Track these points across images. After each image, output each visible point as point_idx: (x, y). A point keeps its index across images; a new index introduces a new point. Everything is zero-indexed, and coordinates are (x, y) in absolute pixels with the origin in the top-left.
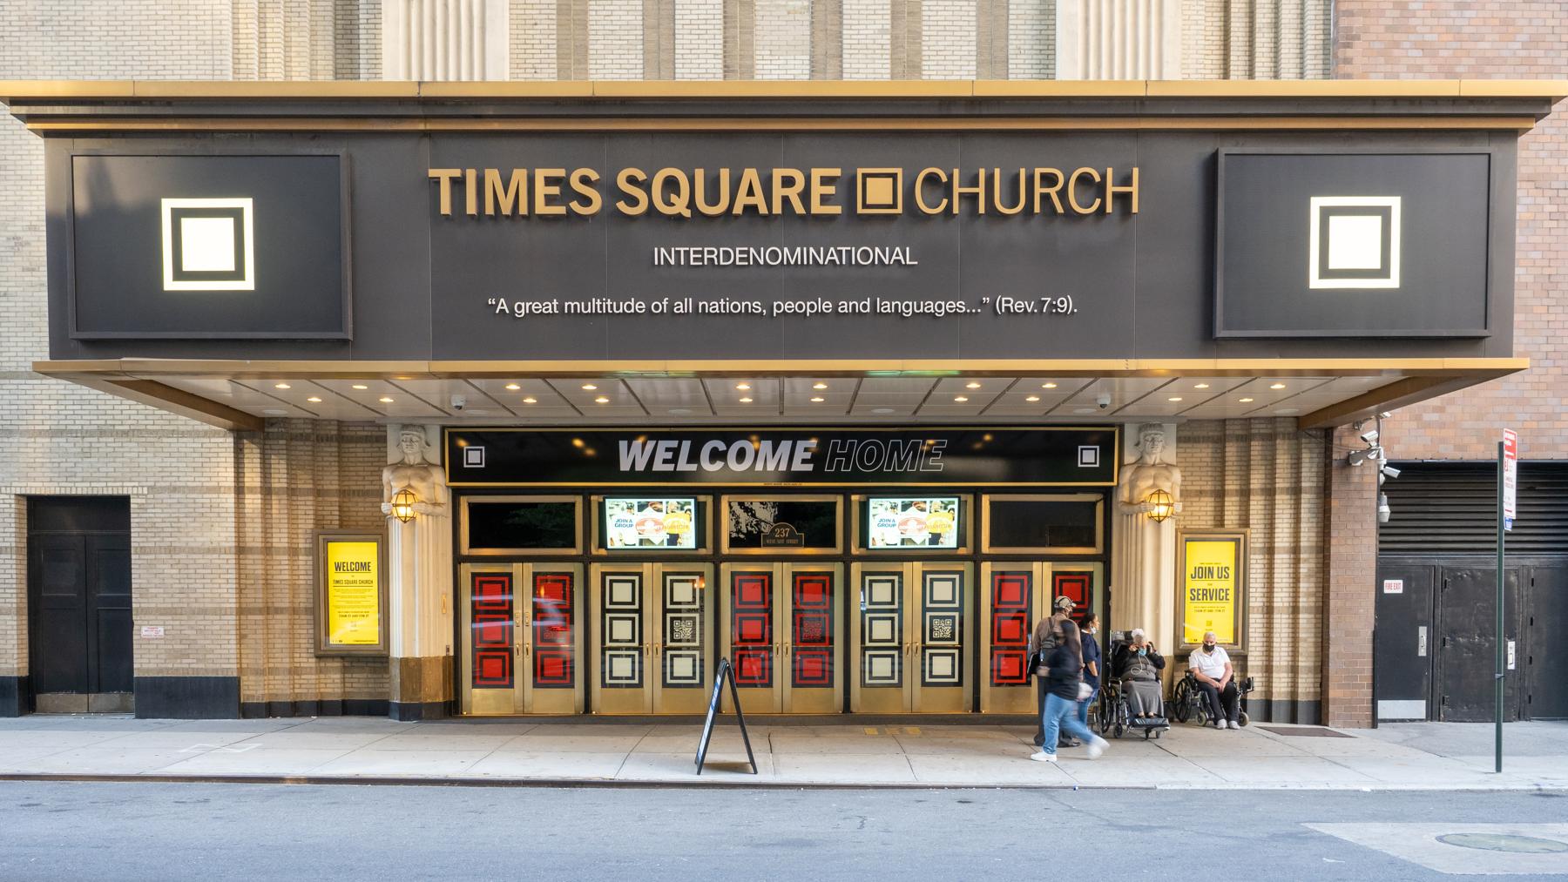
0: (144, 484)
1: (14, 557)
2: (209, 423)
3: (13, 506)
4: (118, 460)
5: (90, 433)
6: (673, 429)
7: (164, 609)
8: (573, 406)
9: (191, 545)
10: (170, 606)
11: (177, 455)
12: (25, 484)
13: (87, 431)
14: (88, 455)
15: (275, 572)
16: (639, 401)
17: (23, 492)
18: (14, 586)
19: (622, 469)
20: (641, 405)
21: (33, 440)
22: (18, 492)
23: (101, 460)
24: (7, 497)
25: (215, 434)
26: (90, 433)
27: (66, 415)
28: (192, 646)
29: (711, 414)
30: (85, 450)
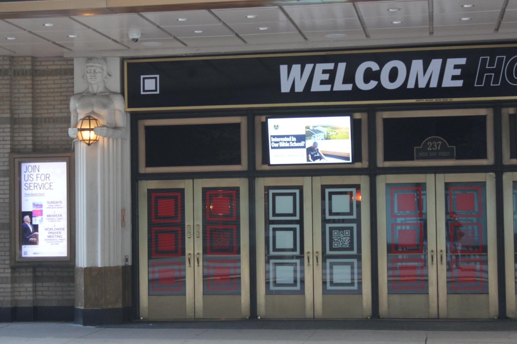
6: (328, 53)
8: (237, 35)
16: (297, 27)
19: (283, 90)
20: (300, 32)
29: (365, 37)
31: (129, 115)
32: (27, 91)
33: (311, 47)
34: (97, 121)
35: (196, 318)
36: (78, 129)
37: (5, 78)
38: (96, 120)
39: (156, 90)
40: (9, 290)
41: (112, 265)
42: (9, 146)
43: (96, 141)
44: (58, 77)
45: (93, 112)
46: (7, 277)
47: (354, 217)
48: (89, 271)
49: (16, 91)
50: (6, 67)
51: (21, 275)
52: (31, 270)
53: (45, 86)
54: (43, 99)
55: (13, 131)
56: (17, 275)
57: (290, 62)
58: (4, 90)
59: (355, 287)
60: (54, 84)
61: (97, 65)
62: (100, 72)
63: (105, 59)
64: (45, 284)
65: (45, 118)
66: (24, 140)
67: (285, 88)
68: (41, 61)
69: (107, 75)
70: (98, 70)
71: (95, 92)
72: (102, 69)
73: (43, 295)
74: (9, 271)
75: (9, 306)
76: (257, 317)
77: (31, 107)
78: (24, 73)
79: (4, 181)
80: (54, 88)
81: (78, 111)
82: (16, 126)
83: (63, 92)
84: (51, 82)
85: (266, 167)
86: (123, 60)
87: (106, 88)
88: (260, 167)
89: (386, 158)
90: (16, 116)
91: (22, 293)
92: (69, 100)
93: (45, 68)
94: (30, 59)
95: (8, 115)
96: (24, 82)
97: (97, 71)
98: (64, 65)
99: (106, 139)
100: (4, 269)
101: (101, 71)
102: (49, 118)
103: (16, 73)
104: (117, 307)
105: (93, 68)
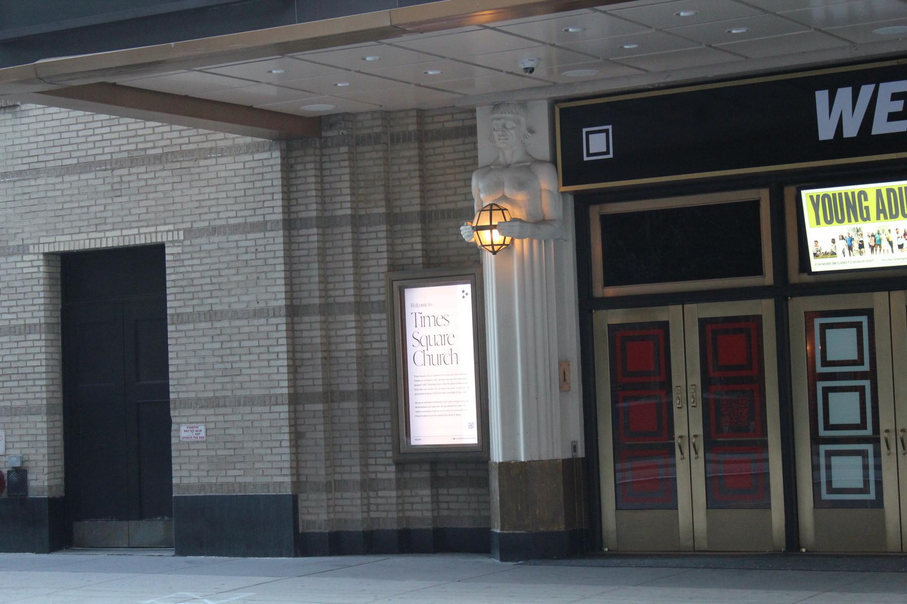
0: (178, 227)
1: (43, 337)
2: (245, 134)
3: (42, 269)
4: (151, 196)
5: (119, 164)
7: (206, 399)
9: (235, 307)
10: (211, 394)
11: (216, 182)
12: (52, 239)
13: (117, 161)
14: (118, 193)
15: (339, 340)
17: (52, 250)
18: (44, 376)
21: (60, 179)
22: (46, 251)
23: (133, 198)
24: (35, 257)
25: (257, 149)
26: (119, 164)
27: (94, 142)
28: (238, 452)
30: (116, 186)
31: (570, 199)
32: (412, 167)
33: (864, 55)
34: (505, 211)
35: (696, 549)
36: (473, 227)
37: (379, 147)
38: (503, 210)
39: (607, 153)
40: (394, 501)
41: (544, 457)
42: (385, 262)
43: (509, 247)
44: (460, 141)
45: (504, 198)
46: (390, 480)
47: (866, 367)
48: (505, 467)
49: (396, 168)
50: (378, 130)
51: (415, 475)
52: (426, 466)
53: (441, 158)
54: (439, 179)
55: (391, 235)
56: (407, 475)
57: (832, 84)
58: (376, 169)
59: (872, 496)
60: (455, 152)
61: (508, 115)
62: (513, 128)
63: (523, 105)
64: (451, 491)
65: (443, 211)
66: (409, 251)
67: (826, 132)
68: (433, 116)
69: (526, 131)
70: (510, 124)
71: (509, 163)
72: (518, 122)
73: (448, 509)
74: (393, 468)
75: (395, 527)
76: (799, 547)
77: (418, 194)
78: (406, 138)
79: (380, 320)
80: (454, 160)
81: (482, 196)
82: (398, 227)
83: (468, 165)
84: (450, 149)
85: (805, 278)
86: (553, 103)
87: (527, 154)
88: (795, 277)
89: (758, 270)
90: (397, 211)
91: (415, 506)
92: (470, 179)
93: (440, 126)
94: (414, 113)
95: (349, 212)
96: (408, 153)
97: (508, 127)
98: (469, 119)
99: (526, 241)
100: (385, 465)
101: (514, 125)
102: (449, 211)
103: (395, 139)
104: (556, 529)
105: (501, 122)
